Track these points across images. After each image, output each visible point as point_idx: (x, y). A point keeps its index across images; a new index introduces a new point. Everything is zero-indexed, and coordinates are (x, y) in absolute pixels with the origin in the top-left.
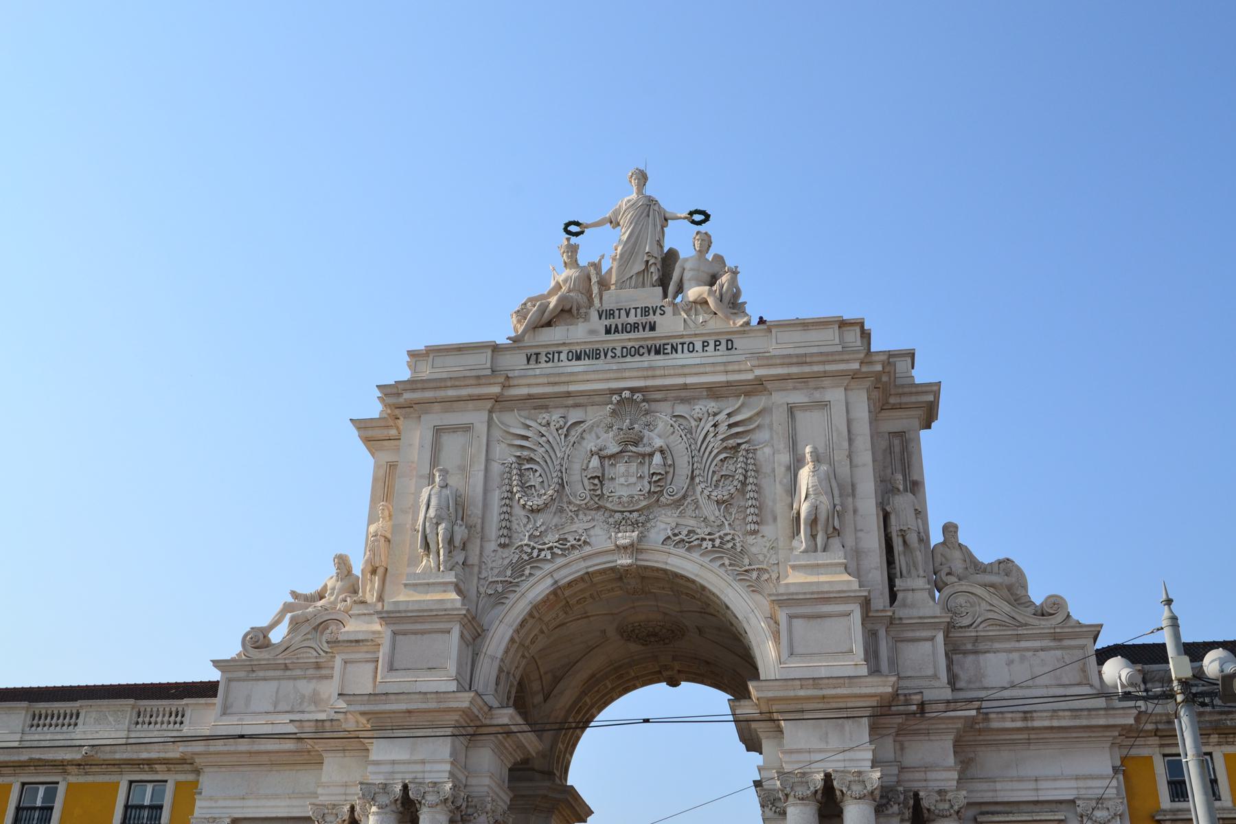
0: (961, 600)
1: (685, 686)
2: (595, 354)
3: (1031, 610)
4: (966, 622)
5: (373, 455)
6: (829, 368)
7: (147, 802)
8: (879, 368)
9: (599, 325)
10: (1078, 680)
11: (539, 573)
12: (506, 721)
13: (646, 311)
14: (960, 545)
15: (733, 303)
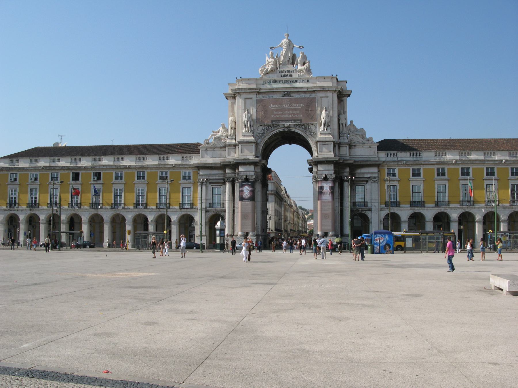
0: (353, 137)
1: (293, 145)
2: (279, 82)
3: (366, 140)
4: (353, 142)
5: (227, 99)
6: (329, 89)
7: (187, 175)
8: (339, 89)
9: (280, 74)
10: (373, 154)
11: (269, 131)
12: (264, 163)
13: (289, 71)
14: (353, 125)
15: (309, 71)
